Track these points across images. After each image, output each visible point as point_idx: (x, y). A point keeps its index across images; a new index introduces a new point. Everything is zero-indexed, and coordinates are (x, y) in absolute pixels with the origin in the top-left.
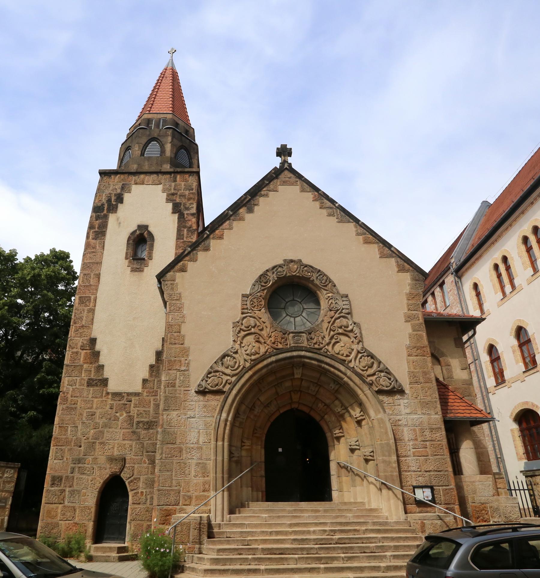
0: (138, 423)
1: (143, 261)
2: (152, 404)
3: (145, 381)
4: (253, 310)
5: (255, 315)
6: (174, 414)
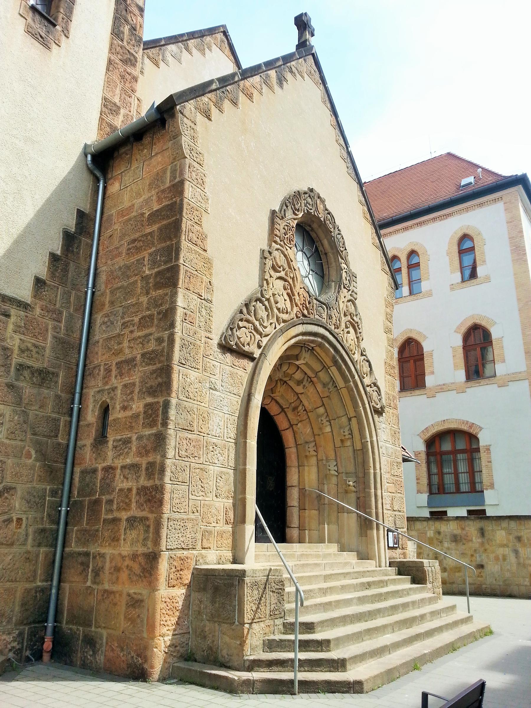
0: (21, 367)
1: (51, 27)
2: (50, 335)
3: (39, 282)
6: (193, 375)
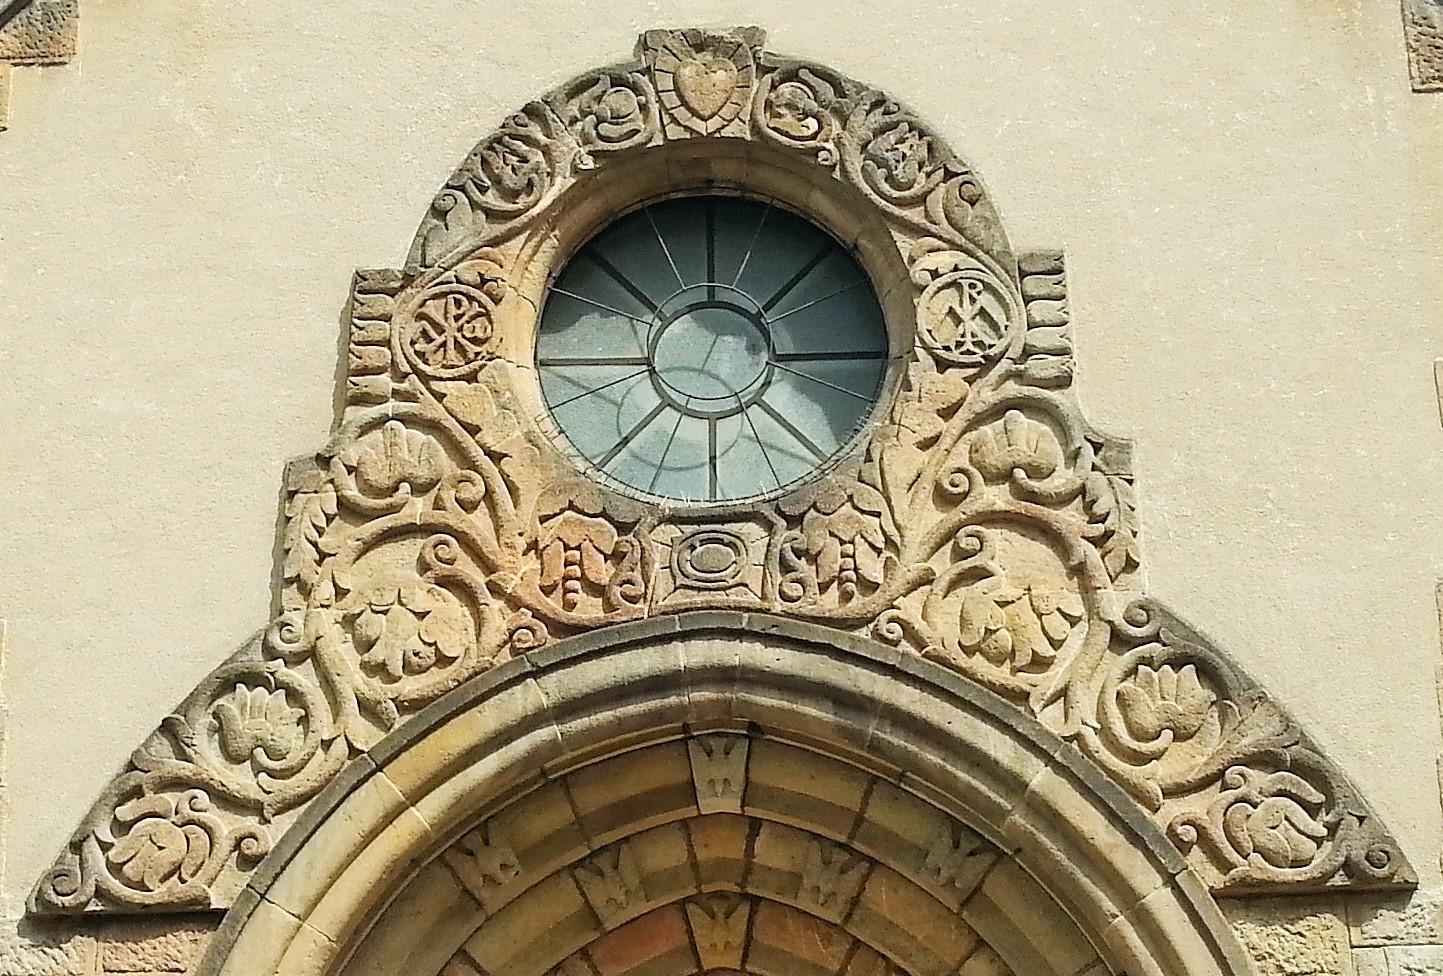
4: (425, 378)
5: (434, 410)
